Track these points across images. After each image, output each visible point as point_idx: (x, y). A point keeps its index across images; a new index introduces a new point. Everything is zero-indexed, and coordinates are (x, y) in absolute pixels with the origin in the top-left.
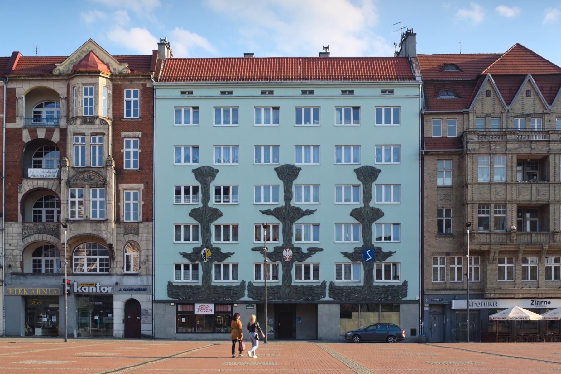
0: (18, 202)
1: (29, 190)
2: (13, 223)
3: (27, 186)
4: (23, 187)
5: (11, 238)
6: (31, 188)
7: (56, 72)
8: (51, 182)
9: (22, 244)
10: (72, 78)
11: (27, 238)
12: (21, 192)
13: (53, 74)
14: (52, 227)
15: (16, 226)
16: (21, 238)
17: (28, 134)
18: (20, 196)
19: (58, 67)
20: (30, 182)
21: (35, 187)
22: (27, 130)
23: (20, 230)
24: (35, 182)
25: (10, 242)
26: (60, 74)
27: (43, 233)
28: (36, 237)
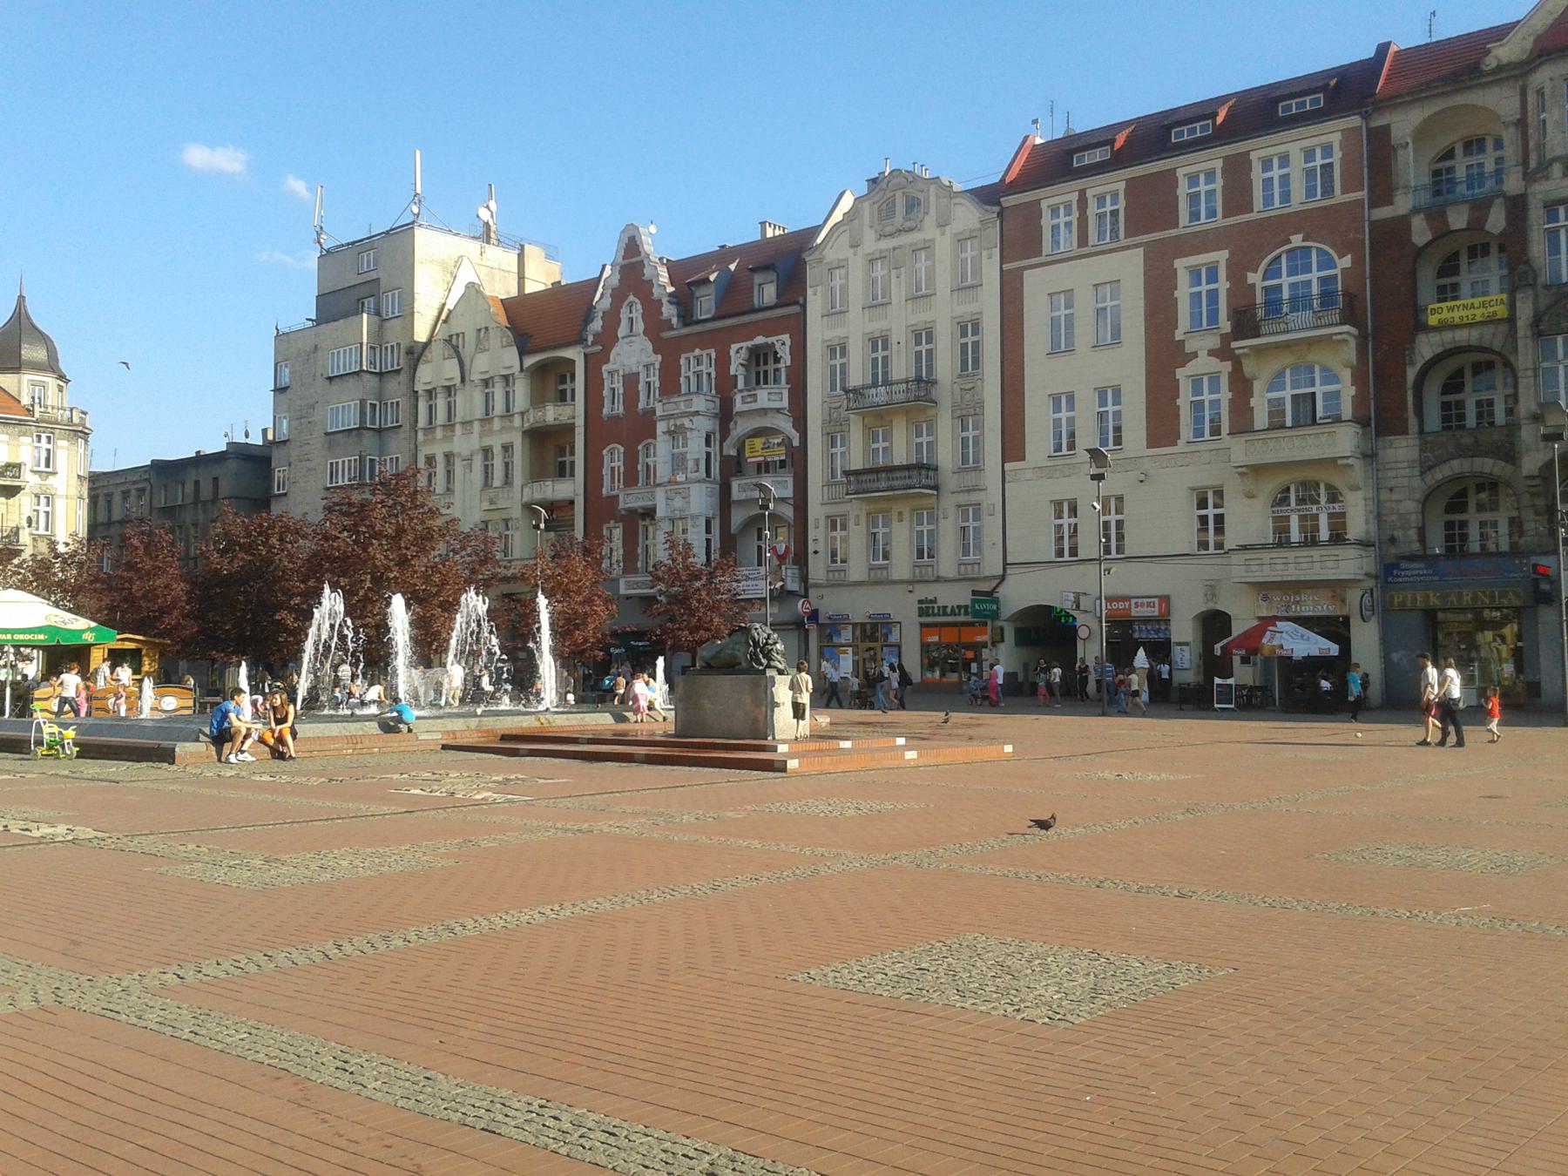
0: (1405, 387)
1: (1432, 355)
2: (1398, 437)
3: (1426, 347)
4: (1417, 351)
5: (1391, 474)
6: (1439, 350)
7: (1490, 62)
8: (1488, 331)
9: (1419, 486)
10: (1533, 70)
11: (1432, 471)
12: (1413, 363)
13: (1482, 71)
14: (1495, 438)
15: (1404, 443)
16: (1416, 472)
17: (1424, 224)
18: (1411, 374)
19: (1494, 52)
20: (1435, 338)
21: (1449, 347)
22: (1422, 216)
23: (1414, 453)
24: (1448, 336)
25: (1392, 483)
26: (1500, 68)
27: (1472, 456)
28: (1456, 466)
